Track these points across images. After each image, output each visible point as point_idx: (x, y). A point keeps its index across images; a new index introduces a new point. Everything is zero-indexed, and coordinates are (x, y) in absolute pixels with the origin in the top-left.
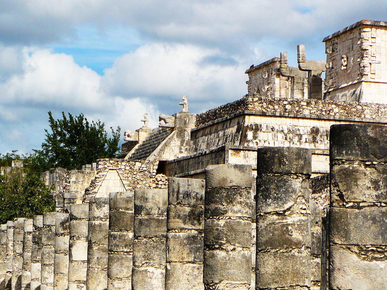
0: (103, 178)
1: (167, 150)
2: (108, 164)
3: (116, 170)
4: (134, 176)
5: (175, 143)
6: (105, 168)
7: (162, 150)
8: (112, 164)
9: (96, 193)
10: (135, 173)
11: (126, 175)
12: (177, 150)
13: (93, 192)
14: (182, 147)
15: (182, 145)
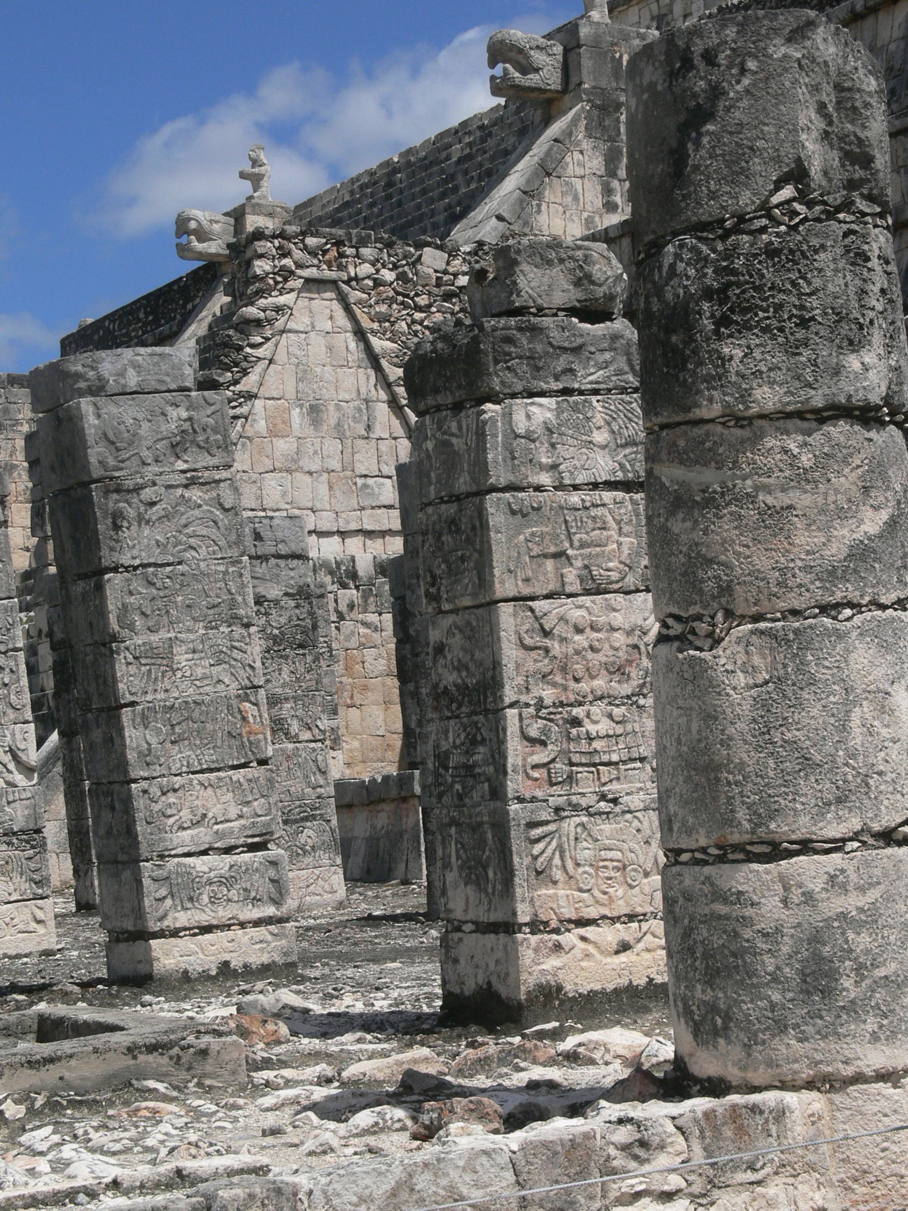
0: (279, 324)
1: (552, 193)
2: (298, 254)
3: (334, 282)
4: (418, 316)
5: (585, 162)
6: (287, 274)
7: (530, 193)
8: (313, 253)
9: (250, 396)
10: (422, 301)
11: (383, 308)
12: (592, 196)
13: (240, 394)
14: (615, 184)
15: (611, 173)
